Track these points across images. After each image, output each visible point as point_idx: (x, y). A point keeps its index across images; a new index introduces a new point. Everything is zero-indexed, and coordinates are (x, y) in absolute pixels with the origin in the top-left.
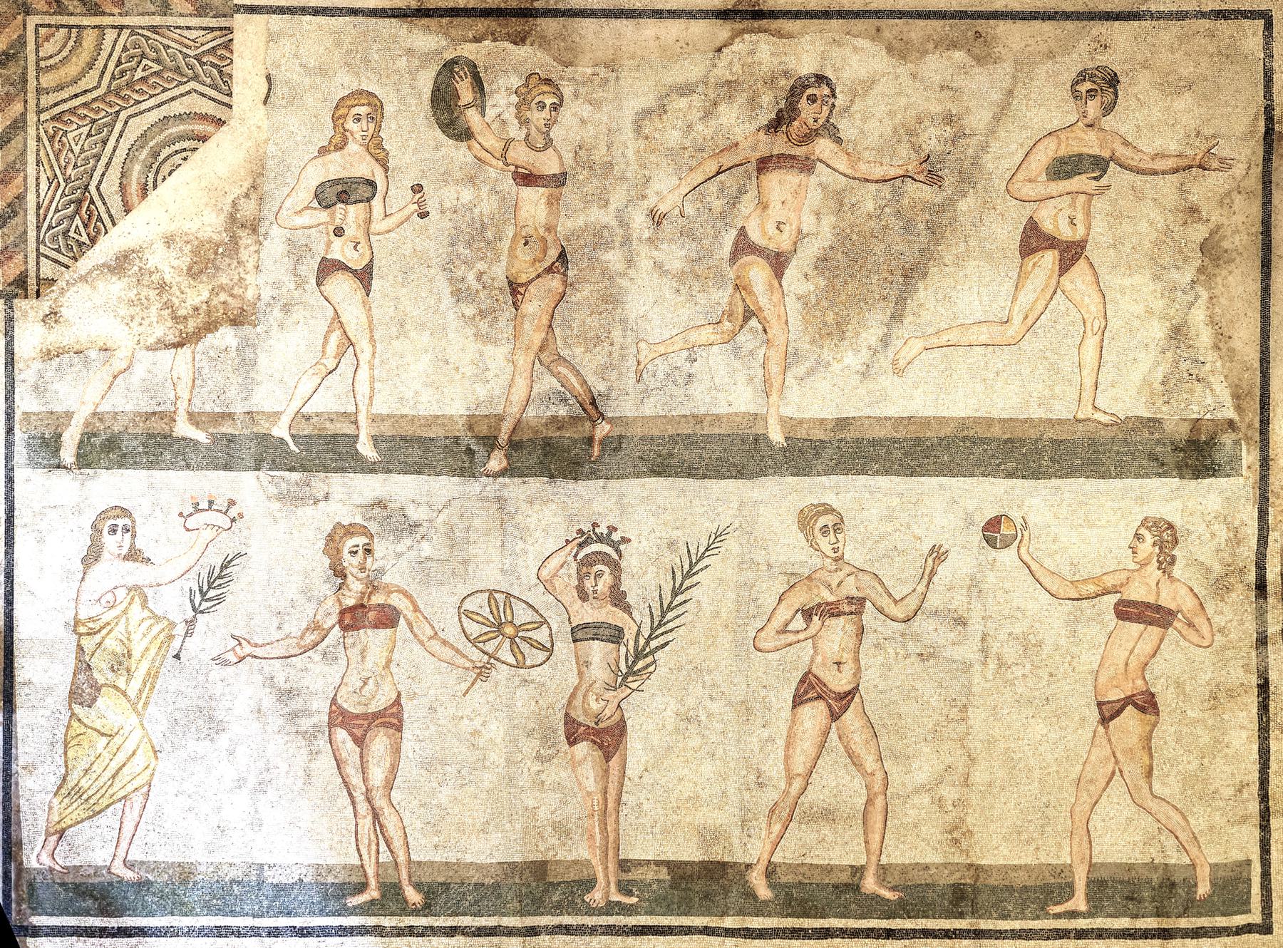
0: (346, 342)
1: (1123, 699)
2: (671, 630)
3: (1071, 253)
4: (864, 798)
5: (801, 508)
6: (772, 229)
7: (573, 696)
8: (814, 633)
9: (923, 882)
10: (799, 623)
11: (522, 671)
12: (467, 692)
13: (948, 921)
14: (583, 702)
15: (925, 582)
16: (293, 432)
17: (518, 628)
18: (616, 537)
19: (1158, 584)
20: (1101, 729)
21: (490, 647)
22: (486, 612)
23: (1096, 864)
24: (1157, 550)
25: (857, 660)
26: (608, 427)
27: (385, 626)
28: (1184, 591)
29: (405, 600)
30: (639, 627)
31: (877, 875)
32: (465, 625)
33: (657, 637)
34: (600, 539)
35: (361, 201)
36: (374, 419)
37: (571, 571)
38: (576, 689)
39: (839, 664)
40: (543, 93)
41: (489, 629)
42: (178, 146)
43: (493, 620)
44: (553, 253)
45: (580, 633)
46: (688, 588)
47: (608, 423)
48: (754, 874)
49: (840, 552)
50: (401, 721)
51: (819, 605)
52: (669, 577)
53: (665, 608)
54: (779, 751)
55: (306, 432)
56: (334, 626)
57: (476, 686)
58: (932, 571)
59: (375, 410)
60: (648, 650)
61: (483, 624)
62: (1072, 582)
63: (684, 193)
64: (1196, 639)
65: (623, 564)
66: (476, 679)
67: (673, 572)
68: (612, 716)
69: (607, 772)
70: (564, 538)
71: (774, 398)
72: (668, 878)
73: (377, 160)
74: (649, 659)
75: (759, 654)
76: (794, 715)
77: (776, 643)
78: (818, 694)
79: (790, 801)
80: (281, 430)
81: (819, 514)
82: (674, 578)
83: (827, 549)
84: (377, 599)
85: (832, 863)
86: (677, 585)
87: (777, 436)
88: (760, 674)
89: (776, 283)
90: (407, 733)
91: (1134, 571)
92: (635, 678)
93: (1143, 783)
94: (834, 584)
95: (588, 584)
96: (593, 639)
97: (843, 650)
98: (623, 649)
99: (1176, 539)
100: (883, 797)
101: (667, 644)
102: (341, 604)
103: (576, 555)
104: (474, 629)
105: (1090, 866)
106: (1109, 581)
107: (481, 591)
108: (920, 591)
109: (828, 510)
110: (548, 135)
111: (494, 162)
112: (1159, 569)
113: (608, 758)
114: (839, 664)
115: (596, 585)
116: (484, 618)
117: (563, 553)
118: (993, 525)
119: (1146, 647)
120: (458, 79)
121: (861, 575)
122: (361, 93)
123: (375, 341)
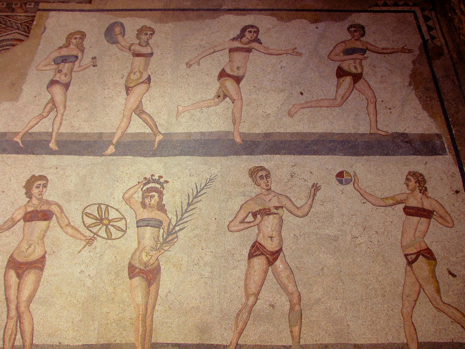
0: (54, 107)
1: (416, 253)
2: (186, 222)
3: (357, 77)
4: (288, 307)
5: (250, 168)
6: (235, 69)
7: (134, 253)
8: (258, 223)
10: (250, 218)
11: (109, 241)
12: (80, 251)
14: (139, 257)
15: (311, 200)
16: (23, 139)
17: (110, 221)
18: (162, 180)
19: (421, 199)
20: (408, 267)
21: (95, 230)
22: (96, 214)
23: (421, 343)
24: (418, 185)
25: (280, 236)
26: (162, 137)
27: (45, 220)
28: (434, 202)
29: (58, 208)
30: (170, 220)
32: (84, 219)
33: (179, 225)
34: (154, 181)
35: (71, 62)
36: (59, 134)
37: (139, 195)
38: (136, 250)
39: (271, 237)
40: (147, 31)
41: (96, 221)
42: (5, 48)
43: (99, 218)
44: (145, 77)
45: (141, 223)
47: (162, 135)
49: (269, 186)
50: (43, 266)
52: (187, 198)
53: (184, 211)
55: (29, 139)
56: (21, 219)
57: (85, 249)
58: (314, 194)
59: (60, 132)
60: (174, 231)
61: (93, 219)
62: (381, 199)
63: (200, 58)
64: (445, 223)
65: (164, 192)
66: (86, 245)
67: (189, 195)
68: (153, 264)
69: (148, 293)
70: (137, 181)
71: (235, 126)
73: (80, 50)
74: (174, 236)
76: (249, 263)
77: (239, 228)
79: (247, 309)
80: (17, 139)
81: (258, 171)
82: (189, 198)
83: (263, 185)
84: (45, 207)
85: (272, 344)
86: (190, 201)
87: (238, 140)
88: (231, 243)
89: (237, 85)
90: (46, 273)
91: (409, 194)
93: (436, 295)
94: (267, 201)
95: (147, 201)
96: (147, 226)
97: (273, 231)
98: (162, 231)
99: (425, 180)
101: (184, 228)
102: (26, 209)
103: (142, 189)
104: (89, 221)
105: (418, 344)
106: (399, 198)
107: (95, 204)
109: (263, 168)
110: (148, 42)
111: (125, 50)
112: (420, 192)
113: (149, 285)
114: (271, 237)
115: (151, 201)
116: (94, 216)
117: (136, 188)
118: (340, 175)
119: (422, 227)
120: (116, 27)
122: (78, 32)
123: (66, 107)
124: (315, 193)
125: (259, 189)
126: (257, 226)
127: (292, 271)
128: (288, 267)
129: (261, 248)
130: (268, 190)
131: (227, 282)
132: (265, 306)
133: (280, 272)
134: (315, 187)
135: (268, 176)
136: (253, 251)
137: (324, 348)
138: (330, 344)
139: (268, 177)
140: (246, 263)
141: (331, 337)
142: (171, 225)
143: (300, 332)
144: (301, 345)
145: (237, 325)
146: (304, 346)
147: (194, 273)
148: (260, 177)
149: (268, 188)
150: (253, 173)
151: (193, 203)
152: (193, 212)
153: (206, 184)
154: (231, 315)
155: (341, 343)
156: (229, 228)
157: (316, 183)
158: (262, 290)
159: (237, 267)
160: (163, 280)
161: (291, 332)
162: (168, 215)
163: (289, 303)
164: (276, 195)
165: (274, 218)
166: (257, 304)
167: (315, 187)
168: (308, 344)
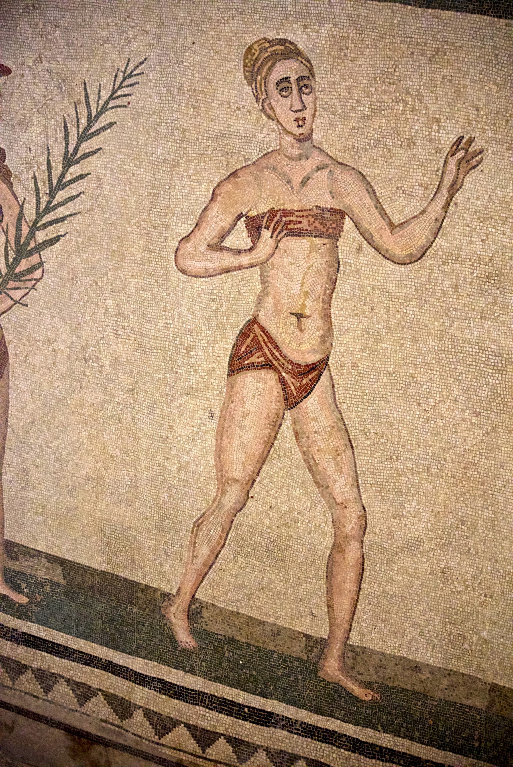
2: (62, 219)
4: (329, 541)
5: (249, 42)
8: (263, 258)
9: (409, 687)
13: (442, 753)
15: (441, 201)
25: (327, 317)
30: (22, 207)
31: (343, 656)
33: (45, 226)
39: (299, 316)
46: (86, 156)
48: (173, 609)
51: (272, 213)
53: (55, 182)
54: (208, 437)
58: (454, 183)
60: (32, 245)
67: (66, 127)
72: (63, 582)
74: (34, 259)
75: (183, 277)
76: (231, 386)
77: (208, 265)
78: (267, 359)
79: (223, 517)
85: (279, 623)
86: (71, 149)
92: (17, 284)
94: (297, 180)
100: (358, 545)
101: (57, 239)
108: (433, 216)
114: (299, 316)
121: (338, 170)
124: (461, 176)
125: (273, 131)
126: (257, 269)
127: (350, 441)
128: (340, 425)
129: (266, 345)
130: (303, 139)
131: (171, 427)
132: (267, 522)
133: (315, 432)
134: (460, 154)
135: (305, 82)
136: (243, 349)
137: (408, 669)
138: (428, 665)
139: (306, 86)
140: (224, 382)
141: (433, 649)
142: (23, 222)
143: (354, 614)
144: (351, 645)
145: (194, 551)
146: (358, 650)
147: (89, 382)
148: (278, 84)
149: (301, 131)
150: (257, 65)
151: (79, 155)
152: (80, 190)
153: (114, 91)
154: (181, 522)
155: (455, 672)
156: (180, 261)
157: (466, 138)
158: (262, 474)
159: (197, 390)
160: (14, 385)
161: (330, 607)
162: (14, 189)
163: (332, 530)
164: (326, 166)
165: (313, 248)
166: (245, 510)
167: (460, 154)
168: (370, 649)
